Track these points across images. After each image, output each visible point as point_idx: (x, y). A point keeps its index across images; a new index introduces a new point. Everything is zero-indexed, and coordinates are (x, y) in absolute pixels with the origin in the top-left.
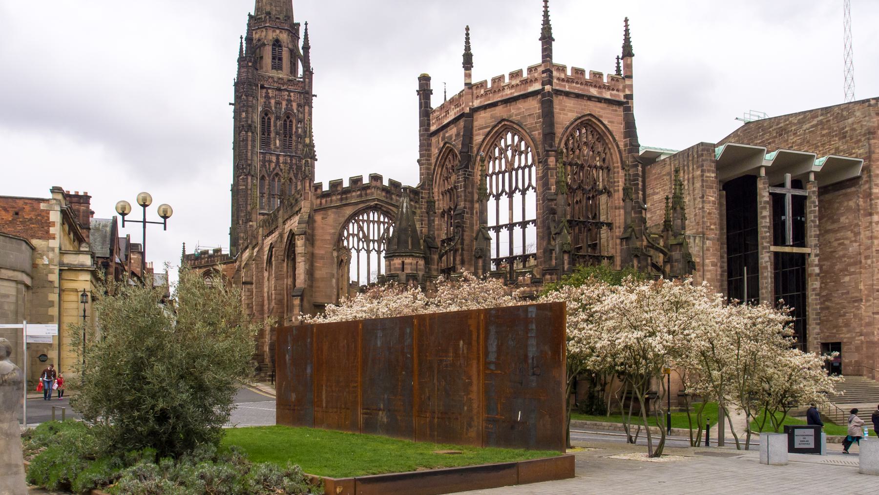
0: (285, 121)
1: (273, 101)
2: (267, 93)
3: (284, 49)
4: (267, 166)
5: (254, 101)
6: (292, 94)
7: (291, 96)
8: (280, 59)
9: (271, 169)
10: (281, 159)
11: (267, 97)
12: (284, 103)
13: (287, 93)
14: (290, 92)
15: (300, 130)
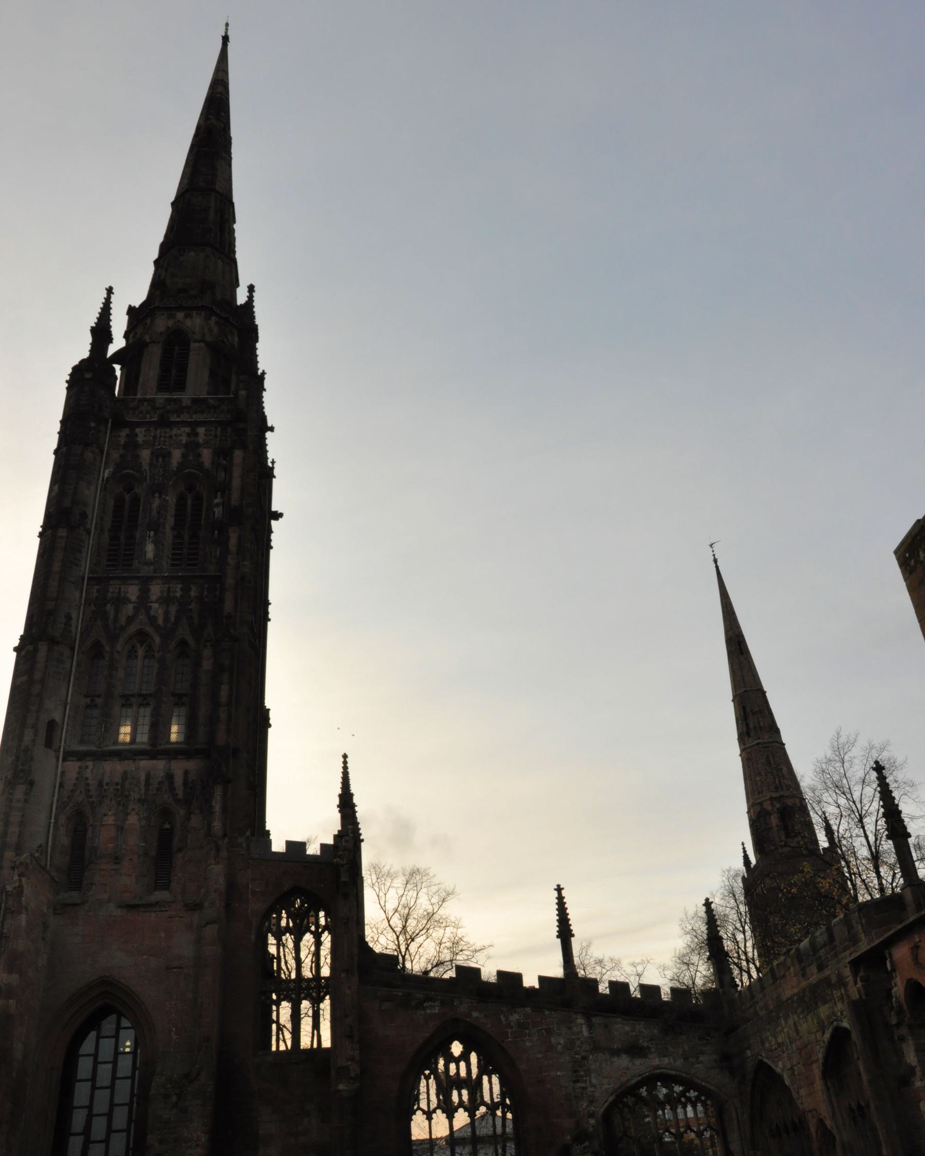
0: (181, 499)
1: (145, 454)
2: (132, 436)
3: (193, 345)
4: (112, 615)
5: (89, 455)
6: (201, 430)
7: (197, 435)
8: (183, 369)
9: (123, 620)
10: (156, 590)
11: (132, 445)
12: (177, 455)
13: (187, 430)
14: (194, 425)
15: (218, 512)
